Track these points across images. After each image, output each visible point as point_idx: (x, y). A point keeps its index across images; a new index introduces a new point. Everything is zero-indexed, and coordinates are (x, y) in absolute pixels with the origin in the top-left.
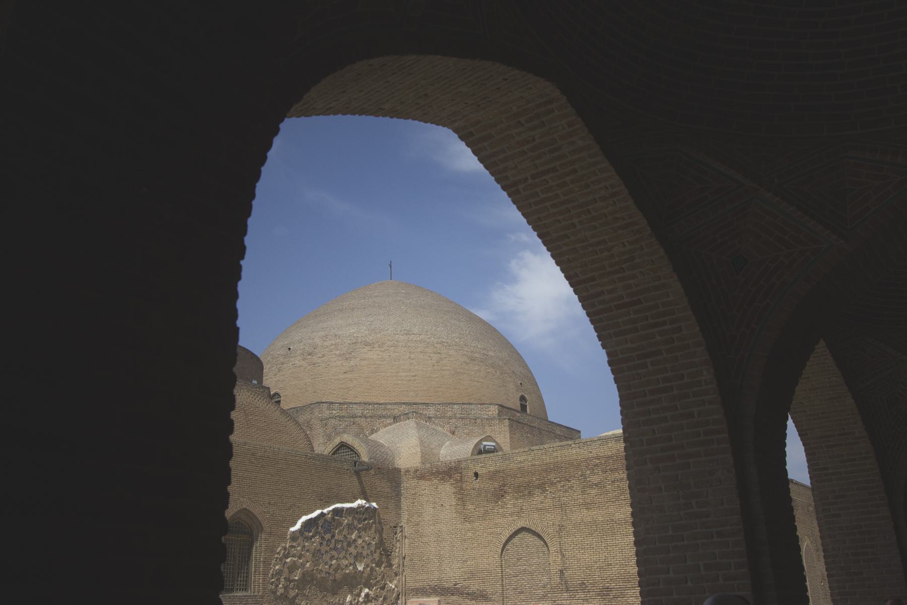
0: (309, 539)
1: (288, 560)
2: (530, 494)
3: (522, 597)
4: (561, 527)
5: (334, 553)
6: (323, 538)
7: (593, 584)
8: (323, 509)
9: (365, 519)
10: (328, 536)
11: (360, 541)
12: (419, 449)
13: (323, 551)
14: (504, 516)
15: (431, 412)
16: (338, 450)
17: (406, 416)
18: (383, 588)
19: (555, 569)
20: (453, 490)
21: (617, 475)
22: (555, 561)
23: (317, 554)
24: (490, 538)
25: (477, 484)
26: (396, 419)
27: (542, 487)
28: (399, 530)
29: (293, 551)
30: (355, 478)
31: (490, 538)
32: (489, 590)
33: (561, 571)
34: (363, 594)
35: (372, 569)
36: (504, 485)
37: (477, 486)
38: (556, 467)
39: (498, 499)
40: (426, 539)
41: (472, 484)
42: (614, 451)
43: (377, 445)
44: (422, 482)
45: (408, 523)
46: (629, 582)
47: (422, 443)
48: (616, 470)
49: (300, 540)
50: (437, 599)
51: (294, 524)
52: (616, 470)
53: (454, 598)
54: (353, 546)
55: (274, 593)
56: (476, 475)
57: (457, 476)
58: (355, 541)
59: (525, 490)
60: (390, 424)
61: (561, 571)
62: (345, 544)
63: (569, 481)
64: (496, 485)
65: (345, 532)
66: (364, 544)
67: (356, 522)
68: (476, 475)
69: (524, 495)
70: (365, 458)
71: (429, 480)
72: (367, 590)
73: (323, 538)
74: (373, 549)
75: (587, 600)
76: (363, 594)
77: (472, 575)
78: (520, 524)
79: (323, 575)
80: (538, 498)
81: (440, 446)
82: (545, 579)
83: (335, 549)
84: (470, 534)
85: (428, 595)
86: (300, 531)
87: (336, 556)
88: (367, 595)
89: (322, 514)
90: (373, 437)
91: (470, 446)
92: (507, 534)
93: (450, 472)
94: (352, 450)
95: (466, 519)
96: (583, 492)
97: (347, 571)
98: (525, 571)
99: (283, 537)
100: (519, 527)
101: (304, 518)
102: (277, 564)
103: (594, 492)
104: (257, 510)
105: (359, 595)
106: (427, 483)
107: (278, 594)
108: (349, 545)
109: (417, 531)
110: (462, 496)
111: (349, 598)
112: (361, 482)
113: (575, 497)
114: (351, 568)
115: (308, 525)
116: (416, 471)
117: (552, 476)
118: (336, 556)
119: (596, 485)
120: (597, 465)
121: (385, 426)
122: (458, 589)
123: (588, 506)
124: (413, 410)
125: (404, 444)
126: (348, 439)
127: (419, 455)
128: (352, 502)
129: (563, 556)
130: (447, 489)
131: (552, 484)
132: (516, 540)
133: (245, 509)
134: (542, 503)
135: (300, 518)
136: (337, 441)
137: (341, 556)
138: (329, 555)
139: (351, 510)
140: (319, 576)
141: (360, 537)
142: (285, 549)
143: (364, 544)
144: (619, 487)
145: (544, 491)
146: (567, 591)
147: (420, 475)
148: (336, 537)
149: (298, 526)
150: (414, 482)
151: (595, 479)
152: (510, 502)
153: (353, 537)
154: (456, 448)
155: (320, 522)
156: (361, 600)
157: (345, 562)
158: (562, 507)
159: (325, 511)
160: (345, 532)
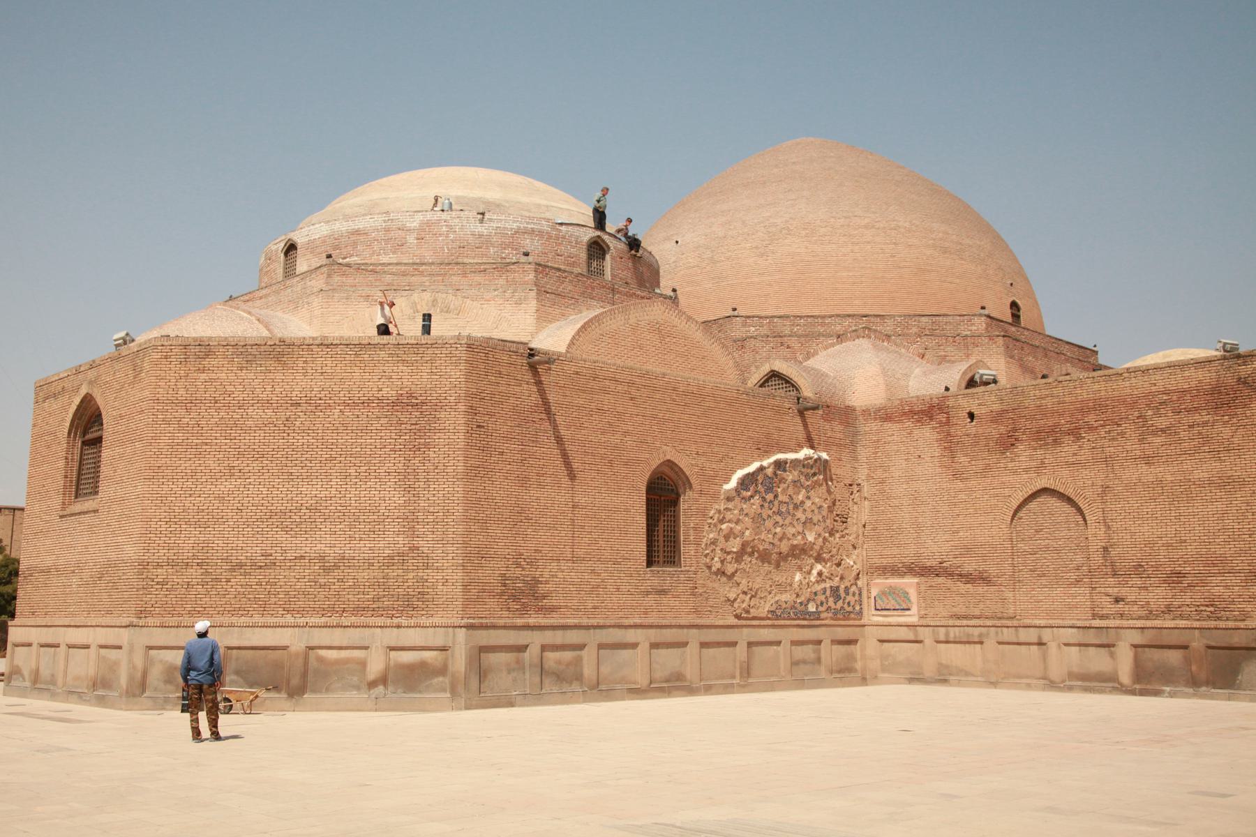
1: (724, 527)
3: (1044, 581)
4: (1106, 489)
5: (778, 518)
6: (764, 499)
7: (1157, 568)
8: (761, 460)
9: (814, 474)
10: (770, 497)
11: (808, 503)
12: (881, 381)
13: (765, 516)
14: (1015, 472)
15: (888, 327)
16: (767, 381)
17: (856, 335)
18: (839, 565)
19: (1096, 545)
20: (936, 436)
21: (1197, 417)
22: (1095, 535)
23: (758, 519)
24: (993, 501)
25: (972, 428)
27: (1075, 433)
28: (855, 488)
29: (729, 516)
30: (798, 420)
31: (993, 501)
33: (1105, 549)
34: (815, 572)
35: (825, 539)
36: (1015, 430)
37: (973, 431)
38: (1098, 406)
39: (1006, 449)
40: (896, 502)
41: (963, 427)
42: (1193, 384)
43: (818, 376)
44: (888, 425)
45: (868, 480)
46: (1215, 565)
47: (884, 372)
48: (1196, 409)
49: (737, 499)
50: (916, 580)
51: (727, 480)
52: (1196, 409)
53: (940, 580)
54: (801, 509)
55: (709, 567)
56: (971, 416)
57: (943, 417)
58: (802, 502)
59: (1048, 436)
60: (833, 345)
62: (791, 507)
63: (1119, 425)
64: (1003, 429)
65: (790, 491)
66: (813, 507)
67: (803, 479)
68: (971, 416)
69: (1047, 444)
70: (807, 392)
71: (899, 422)
72: (819, 567)
73: (764, 499)
74: (825, 513)
75: (1146, 588)
76: (815, 572)
77: (968, 550)
79: (767, 546)
80: (1068, 448)
81: (907, 376)
82: (1079, 559)
83: (779, 513)
84: (962, 496)
85: (902, 575)
86: (736, 490)
87: (781, 522)
88: (820, 574)
89: (762, 469)
90: (810, 363)
91: (953, 376)
92: (1020, 496)
93: (930, 412)
94: (787, 382)
95: (957, 475)
96: (1141, 441)
97: (795, 542)
98: (1047, 547)
99: (715, 497)
100: (1039, 487)
101: (740, 473)
102: (712, 531)
103: (1158, 440)
104: (683, 463)
105: (809, 573)
106: (896, 426)
107: (714, 569)
108: (796, 507)
109: (882, 492)
110: (950, 445)
111: (798, 577)
112: (805, 425)
113: (1129, 448)
114: (800, 537)
115: (745, 482)
117: (1091, 418)
118: (781, 522)
119: (1163, 431)
121: (826, 348)
123: (1148, 460)
124: (867, 325)
125: (860, 373)
126: (781, 366)
127: (883, 387)
128: (796, 452)
130: (927, 434)
131: (1092, 429)
132: (1033, 505)
133: (669, 461)
134: (1075, 454)
135: (734, 472)
136: (766, 369)
137: (787, 522)
138: (772, 522)
139: (795, 462)
140: (761, 548)
141: (808, 498)
142: (719, 512)
143: (813, 507)
144: (1200, 433)
146: (1115, 575)
147: (885, 415)
148: (781, 498)
149: (733, 483)
150: (874, 426)
151: (1162, 422)
152: (1024, 454)
153: (801, 497)
154: (932, 377)
155: (760, 478)
156: (813, 579)
159: (765, 463)
160: (790, 491)
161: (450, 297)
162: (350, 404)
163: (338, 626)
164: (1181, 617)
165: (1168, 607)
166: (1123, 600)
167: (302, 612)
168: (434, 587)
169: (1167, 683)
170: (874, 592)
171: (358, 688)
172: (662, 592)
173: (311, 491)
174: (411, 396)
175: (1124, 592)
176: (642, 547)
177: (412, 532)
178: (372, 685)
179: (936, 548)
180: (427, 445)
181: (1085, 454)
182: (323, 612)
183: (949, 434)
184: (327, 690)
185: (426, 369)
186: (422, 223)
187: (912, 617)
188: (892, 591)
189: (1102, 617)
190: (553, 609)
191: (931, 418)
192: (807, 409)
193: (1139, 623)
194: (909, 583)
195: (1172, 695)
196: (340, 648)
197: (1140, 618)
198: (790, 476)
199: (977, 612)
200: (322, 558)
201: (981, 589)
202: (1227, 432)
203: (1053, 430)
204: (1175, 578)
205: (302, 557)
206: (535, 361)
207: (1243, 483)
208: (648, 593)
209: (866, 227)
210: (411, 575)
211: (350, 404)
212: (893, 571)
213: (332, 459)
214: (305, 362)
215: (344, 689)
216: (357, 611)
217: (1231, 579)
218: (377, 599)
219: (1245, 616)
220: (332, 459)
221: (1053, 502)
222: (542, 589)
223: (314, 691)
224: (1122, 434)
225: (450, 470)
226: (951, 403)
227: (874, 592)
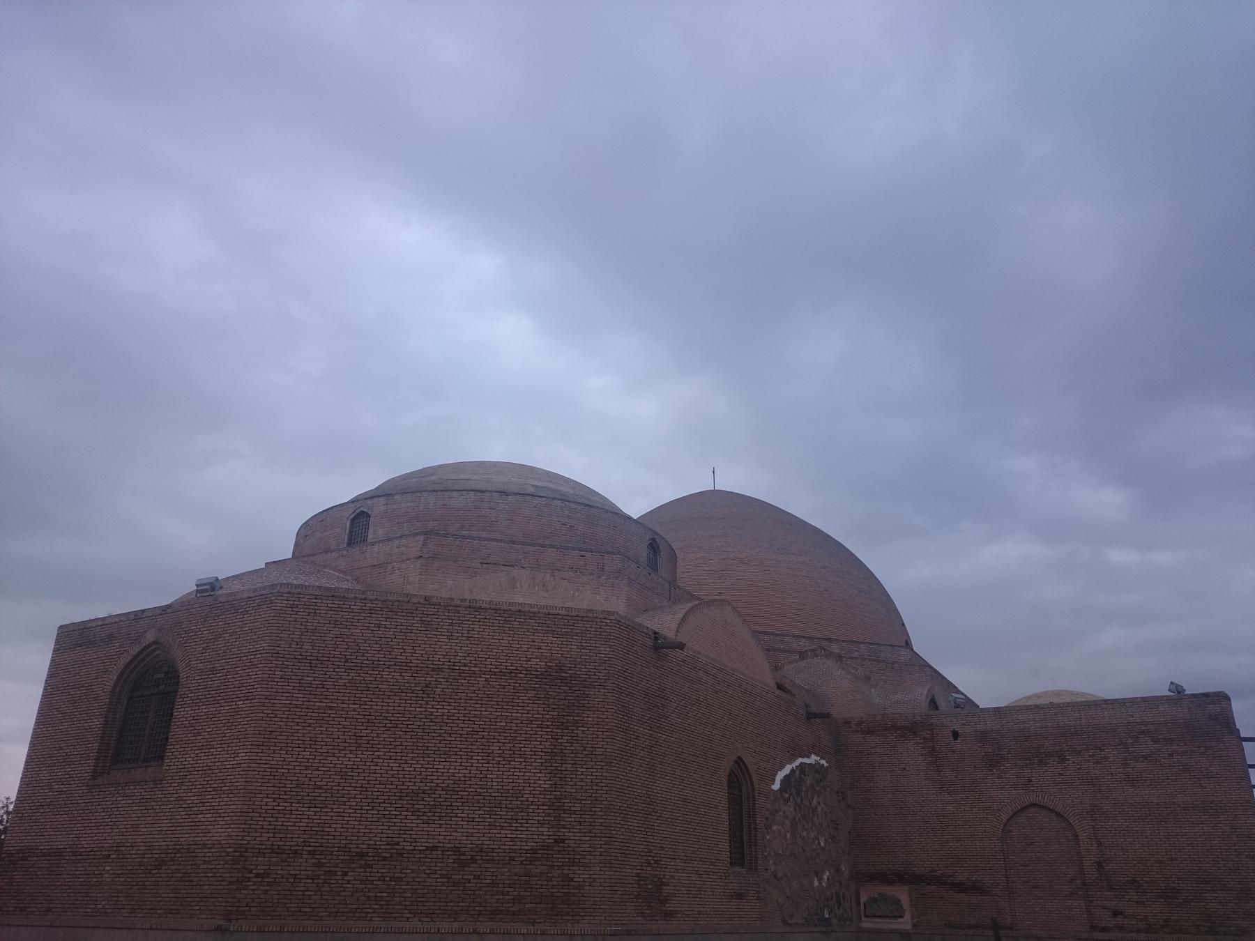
0: (786, 801)
26: (802, 655)
51: (773, 781)
56: (956, 735)
60: (796, 661)
61: (1099, 864)
75: (1143, 903)
83: (804, 817)
85: (891, 883)
89: (793, 771)
96: (1125, 765)
101: (780, 776)
111: (816, 883)
116: (860, 723)
119: (1145, 757)
129: (1100, 844)
145: (1063, 759)
149: (776, 786)
157: (812, 835)
163: (475, 932)
165: (1166, 921)
166: (1121, 913)
170: (864, 898)
172: (740, 896)
183: (934, 750)
187: (905, 923)
189: (1103, 930)
190: (668, 915)
191: (915, 734)
194: (902, 893)
197: (1139, 931)
198: (808, 780)
200: (457, 850)
205: (434, 848)
210: (556, 872)
214: (450, 624)
222: (667, 890)
227: (864, 898)
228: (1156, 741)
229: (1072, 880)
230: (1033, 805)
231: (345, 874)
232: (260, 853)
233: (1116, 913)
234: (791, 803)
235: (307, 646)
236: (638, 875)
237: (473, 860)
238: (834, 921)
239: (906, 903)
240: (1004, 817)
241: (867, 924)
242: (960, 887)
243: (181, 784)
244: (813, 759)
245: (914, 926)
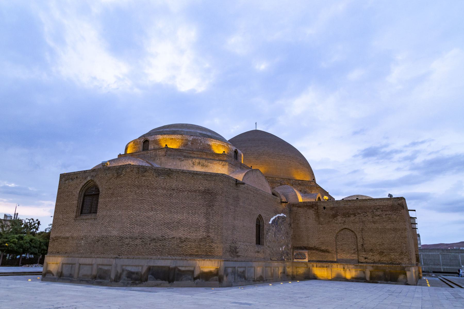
0: (273, 226)
2: (349, 216)
4: (362, 229)
19: (359, 244)
24: (331, 231)
31: (331, 231)
32: (330, 249)
38: (361, 208)
39: (335, 217)
40: (302, 230)
44: (299, 209)
50: (307, 251)
51: (269, 221)
53: (314, 251)
56: (324, 208)
57: (316, 208)
59: (347, 215)
61: (362, 245)
64: (334, 212)
78: (345, 226)
80: (352, 218)
82: (355, 247)
85: (303, 249)
89: (275, 218)
95: (320, 223)
98: (346, 243)
101: (272, 219)
103: (377, 218)
110: (318, 215)
117: (359, 211)
120: (379, 208)
122: (316, 248)
123: (374, 222)
129: (363, 239)
130: (311, 212)
131: (359, 213)
132: (342, 232)
145: (355, 216)
146: (365, 252)
149: (270, 222)
152: (339, 219)
158: (363, 222)
161: (204, 162)
162: (190, 191)
163: (186, 260)
164: (383, 263)
167: (173, 255)
168: (214, 249)
169: (379, 280)
170: (295, 254)
171: (191, 280)
172: (258, 252)
173: (178, 217)
174: (208, 190)
175: (367, 256)
176: (254, 239)
177: (208, 232)
178: (195, 279)
179: (313, 243)
180: (213, 205)
181: (357, 220)
182: (180, 255)
184: (181, 280)
185: (213, 182)
186: (193, 139)
188: (301, 254)
189: (362, 263)
191: (313, 208)
192: (284, 202)
193: (372, 265)
194: (306, 253)
195: (380, 283)
196: (186, 267)
198: (280, 221)
199: (325, 260)
200: (180, 238)
201: (327, 254)
202: (395, 217)
203: (348, 213)
204: (381, 253)
205: (174, 238)
206: (237, 183)
207: (399, 230)
208: (256, 252)
209: (283, 155)
211: (190, 191)
212: (301, 248)
213: (184, 207)
215: (186, 280)
216: (191, 255)
217: (396, 253)
218: (197, 252)
219: (399, 264)
220: (184, 207)
221: (348, 232)
222: (238, 250)
223: (177, 280)
224: (367, 215)
225: (220, 213)
226: (319, 204)
228: (382, 211)
229: (354, 249)
230: (345, 228)
231: (150, 244)
232: (127, 238)
233: (366, 258)
234: (275, 227)
235: (137, 182)
236: (230, 246)
237: (185, 241)
238: (286, 260)
239: (307, 256)
240: (337, 232)
241: (295, 260)
242: (323, 251)
243: (102, 220)
244: (282, 215)
245: (309, 261)
